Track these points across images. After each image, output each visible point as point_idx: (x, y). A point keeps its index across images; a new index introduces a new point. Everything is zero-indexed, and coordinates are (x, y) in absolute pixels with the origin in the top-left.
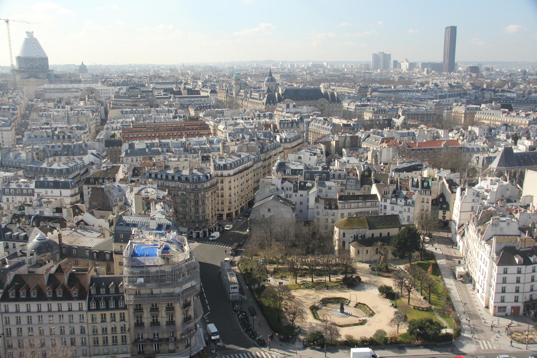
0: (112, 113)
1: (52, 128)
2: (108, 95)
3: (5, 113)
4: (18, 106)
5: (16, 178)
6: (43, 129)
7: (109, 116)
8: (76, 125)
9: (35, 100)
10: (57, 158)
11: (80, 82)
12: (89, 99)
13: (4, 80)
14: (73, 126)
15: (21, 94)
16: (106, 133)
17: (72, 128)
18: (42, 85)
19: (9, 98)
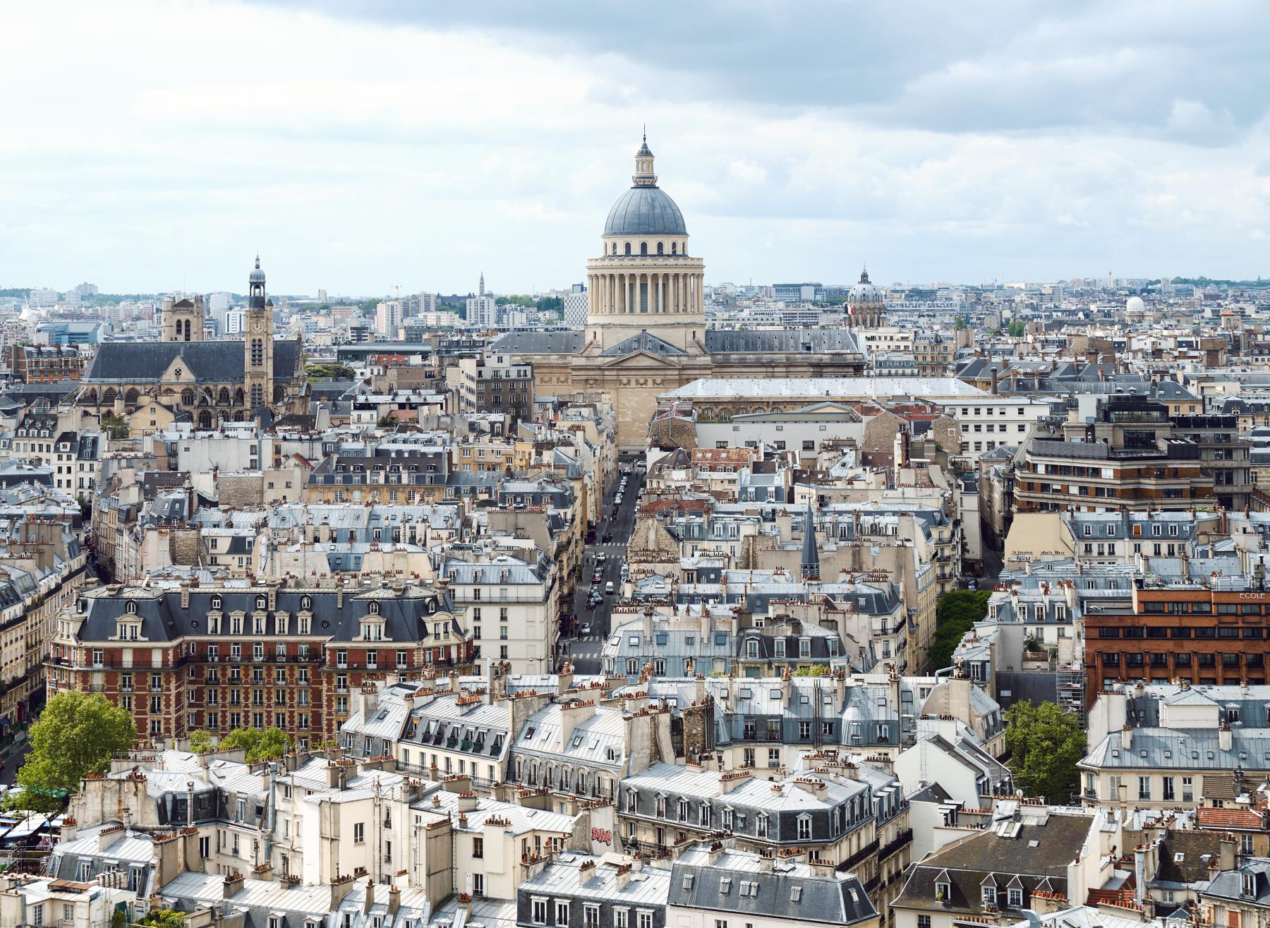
0: (1031, 535)
1: (731, 598)
2: (997, 436)
3: (522, 519)
4: (577, 485)
5: (582, 843)
6: (692, 599)
7: (1014, 543)
8: (847, 588)
9: (654, 455)
10: (761, 754)
11: (858, 369)
12: (907, 456)
13: (517, 359)
14: (829, 589)
15: (590, 426)
16: (1003, 637)
17: (828, 604)
18: (682, 381)
19: (540, 447)
